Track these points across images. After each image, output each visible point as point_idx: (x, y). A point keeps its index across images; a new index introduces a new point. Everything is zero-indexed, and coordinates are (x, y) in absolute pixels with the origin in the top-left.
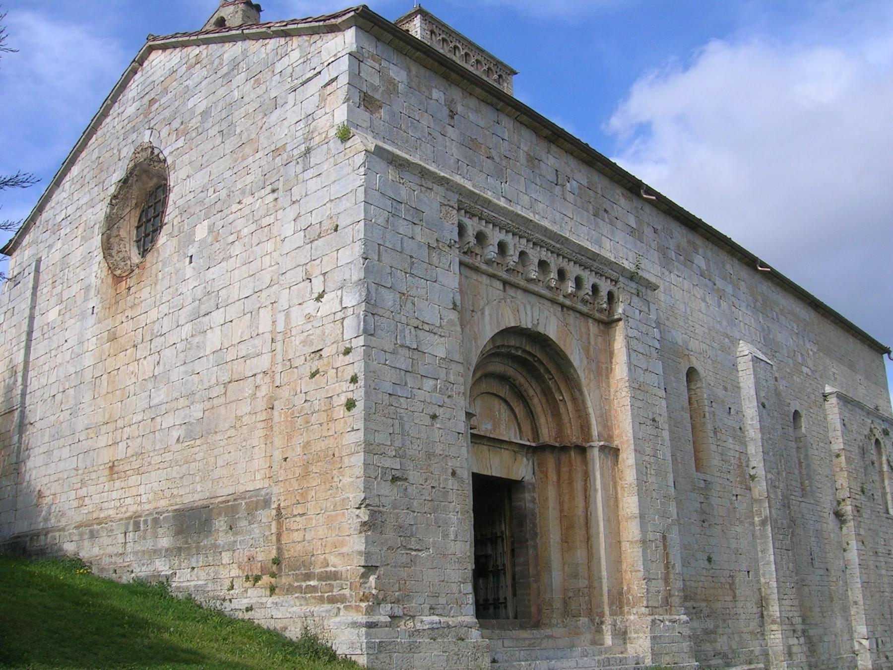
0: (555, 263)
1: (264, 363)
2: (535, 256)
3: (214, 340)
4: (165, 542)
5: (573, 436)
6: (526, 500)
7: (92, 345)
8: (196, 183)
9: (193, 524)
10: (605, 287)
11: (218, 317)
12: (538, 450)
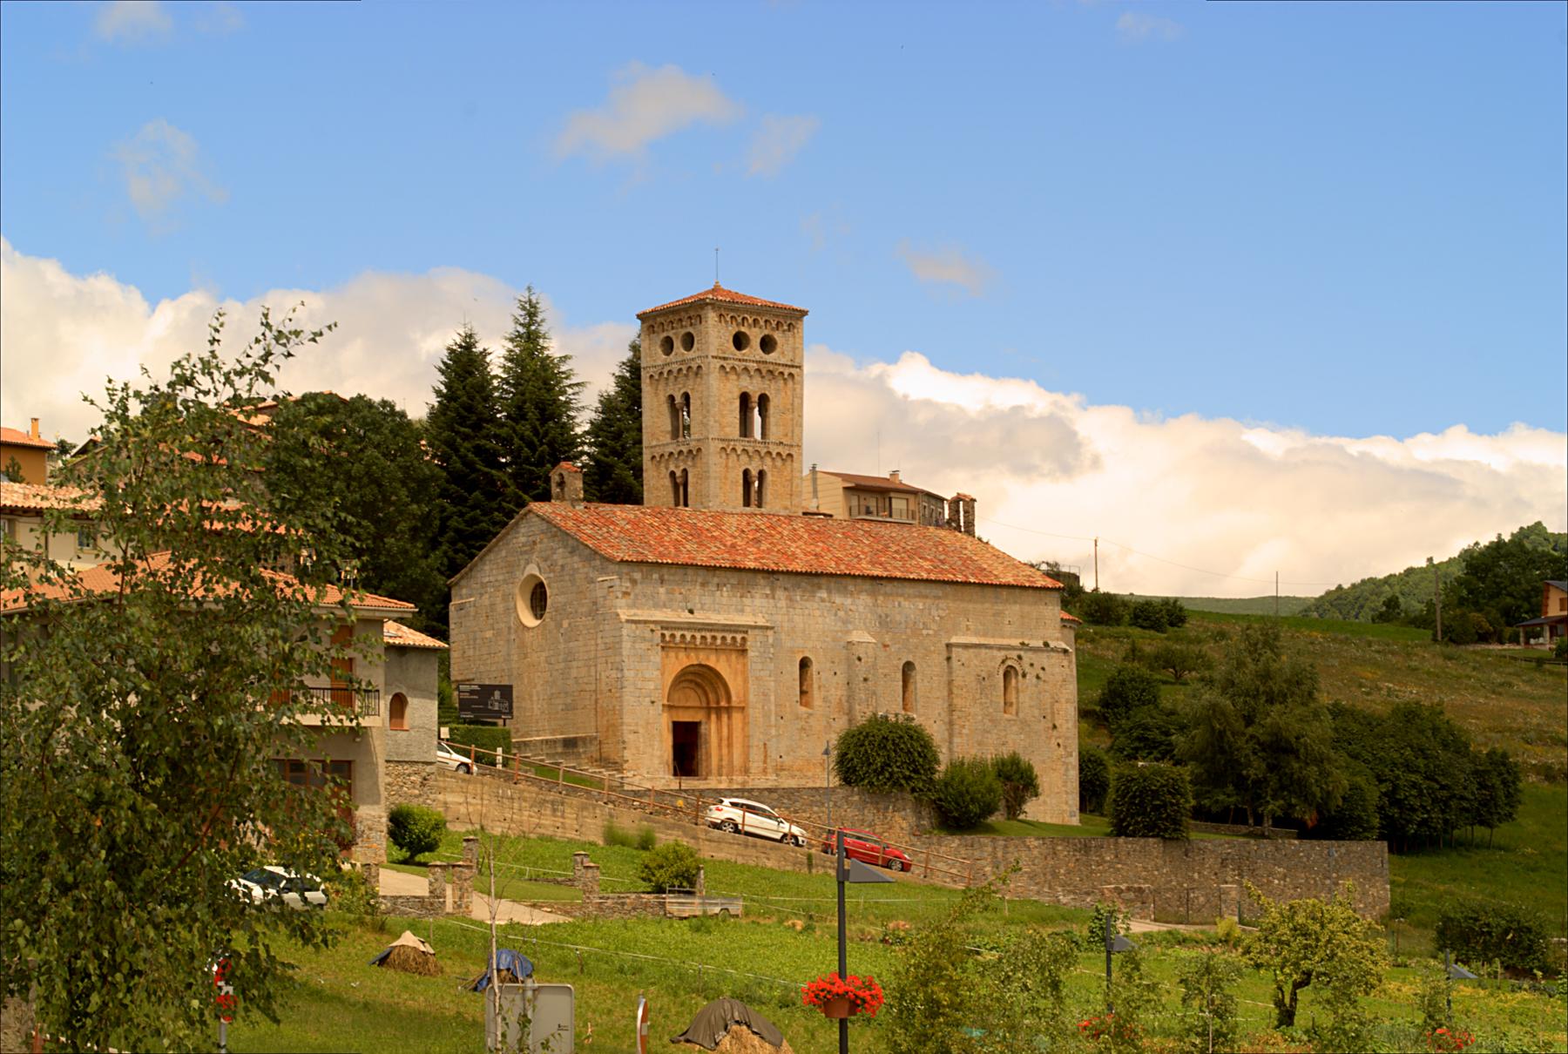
0: (708, 635)
1: (593, 687)
2: (698, 635)
3: (574, 673)
4: (560, 750)
5: (723, 704)
6: (703, 729)
7: (515, 658)
8: (561, 599)
9: (570, 744)
10: (739, 637)
11: (574, 664)
12: (709, 709)
